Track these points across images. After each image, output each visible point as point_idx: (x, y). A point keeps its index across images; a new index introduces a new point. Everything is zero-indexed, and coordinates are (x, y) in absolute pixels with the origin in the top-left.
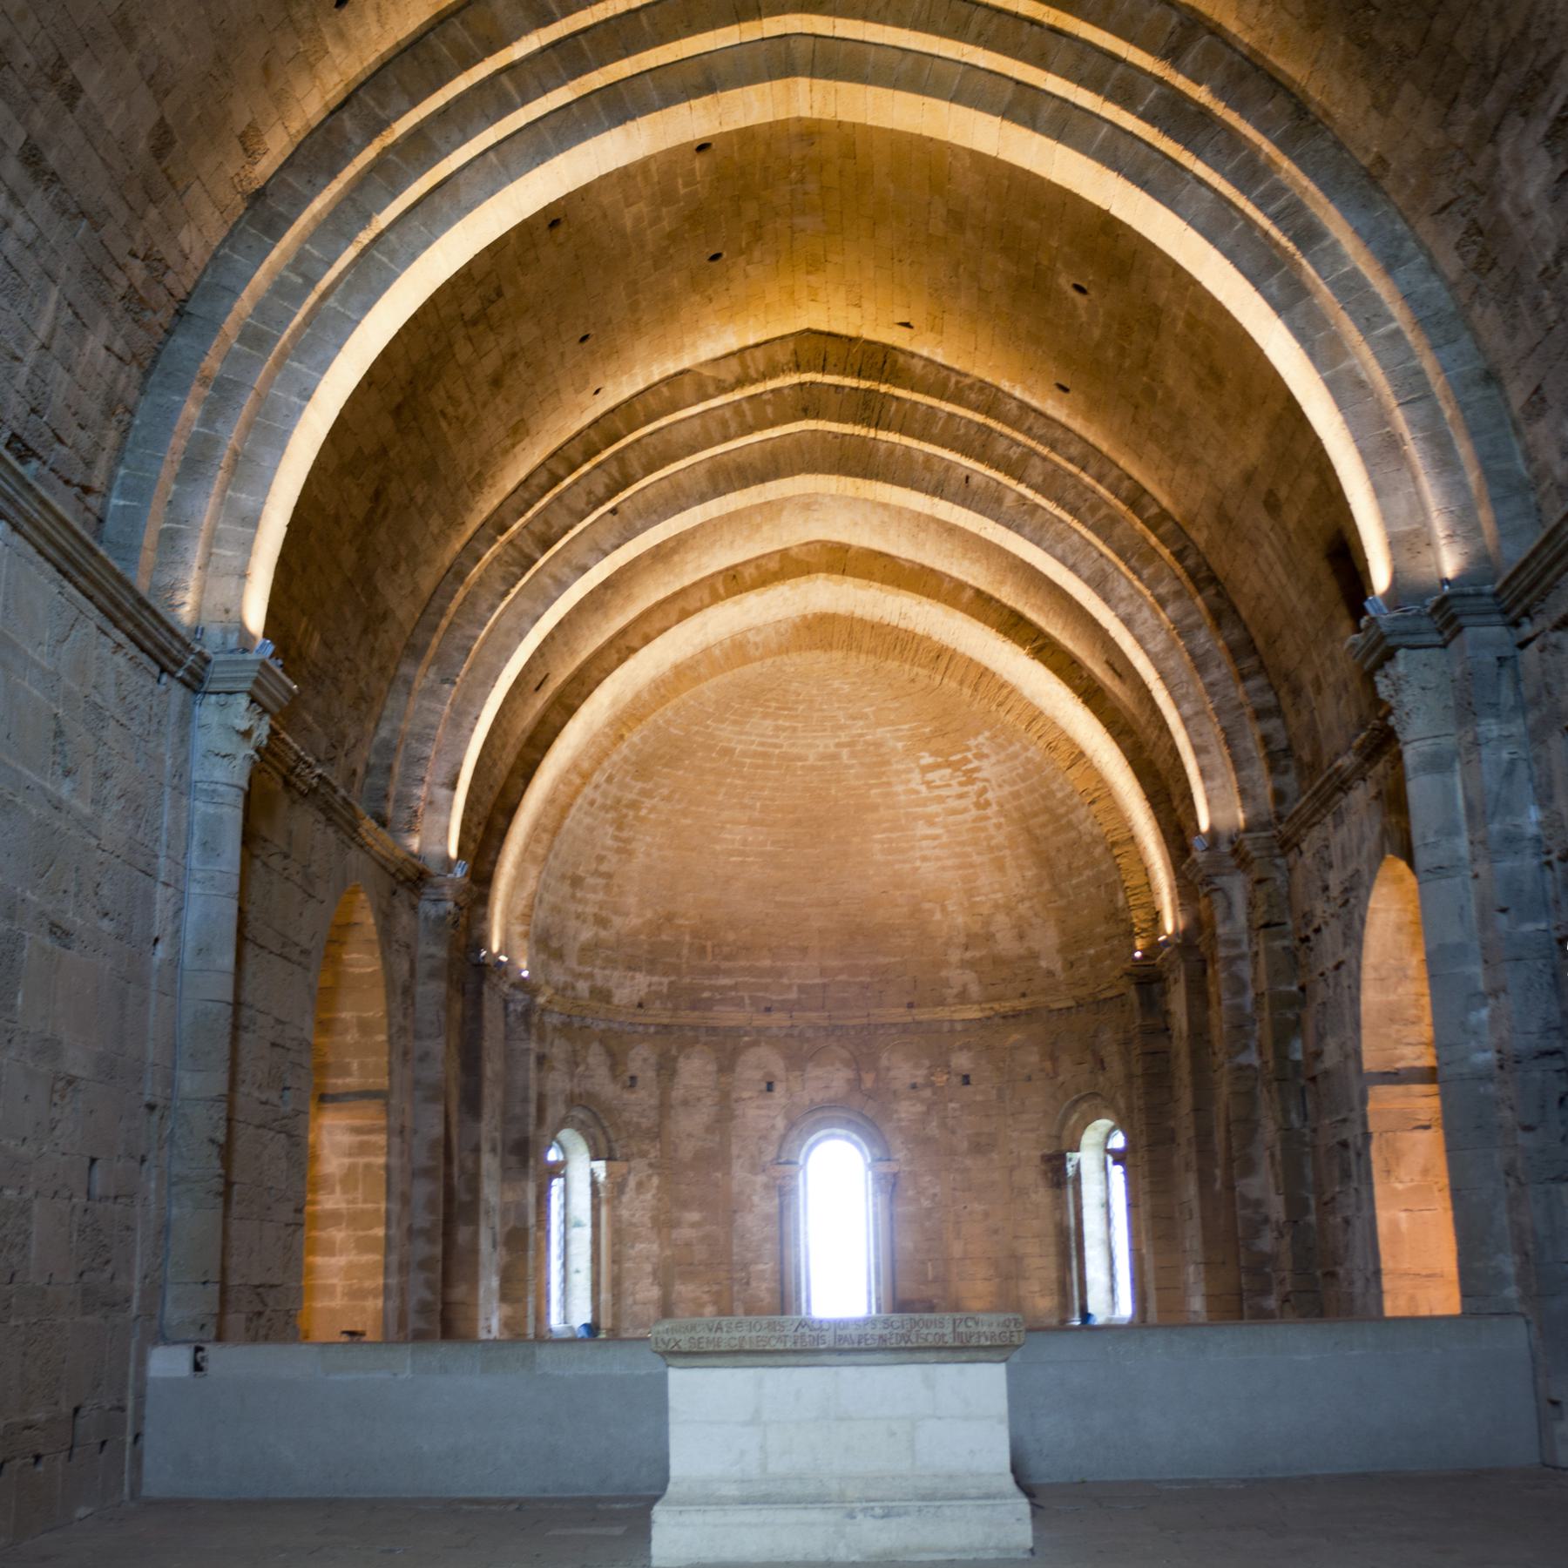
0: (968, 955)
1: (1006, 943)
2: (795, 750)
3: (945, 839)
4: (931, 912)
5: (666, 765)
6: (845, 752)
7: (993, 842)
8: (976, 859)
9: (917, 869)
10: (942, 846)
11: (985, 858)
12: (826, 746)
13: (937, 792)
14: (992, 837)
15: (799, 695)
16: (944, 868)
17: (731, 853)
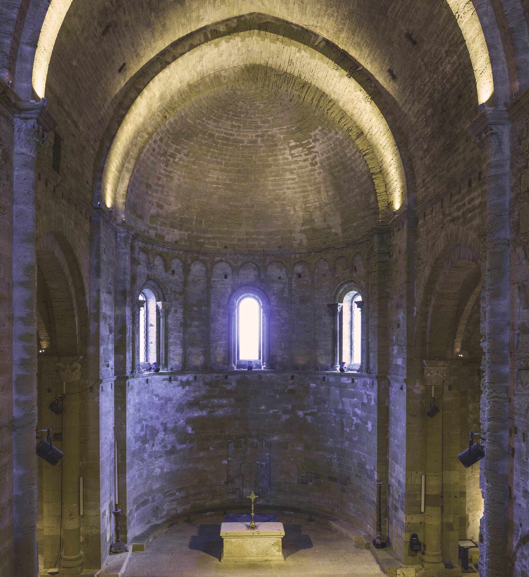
0: (303, 228)
1: (319, 223)
2: (239, 138)
3: (297, 180)
4: (290, 211)
5: (186, 138)
6: (260, 139)
7: (317, 181)
8: (309, 188)
9: (285, 193)
10: (296, 183)
11: (313, 188)
12: (252, 137)
13: (295, 159)
14: (316, 178)
15: (242, 108)
16: (296, 193)
17: (212, 183)
